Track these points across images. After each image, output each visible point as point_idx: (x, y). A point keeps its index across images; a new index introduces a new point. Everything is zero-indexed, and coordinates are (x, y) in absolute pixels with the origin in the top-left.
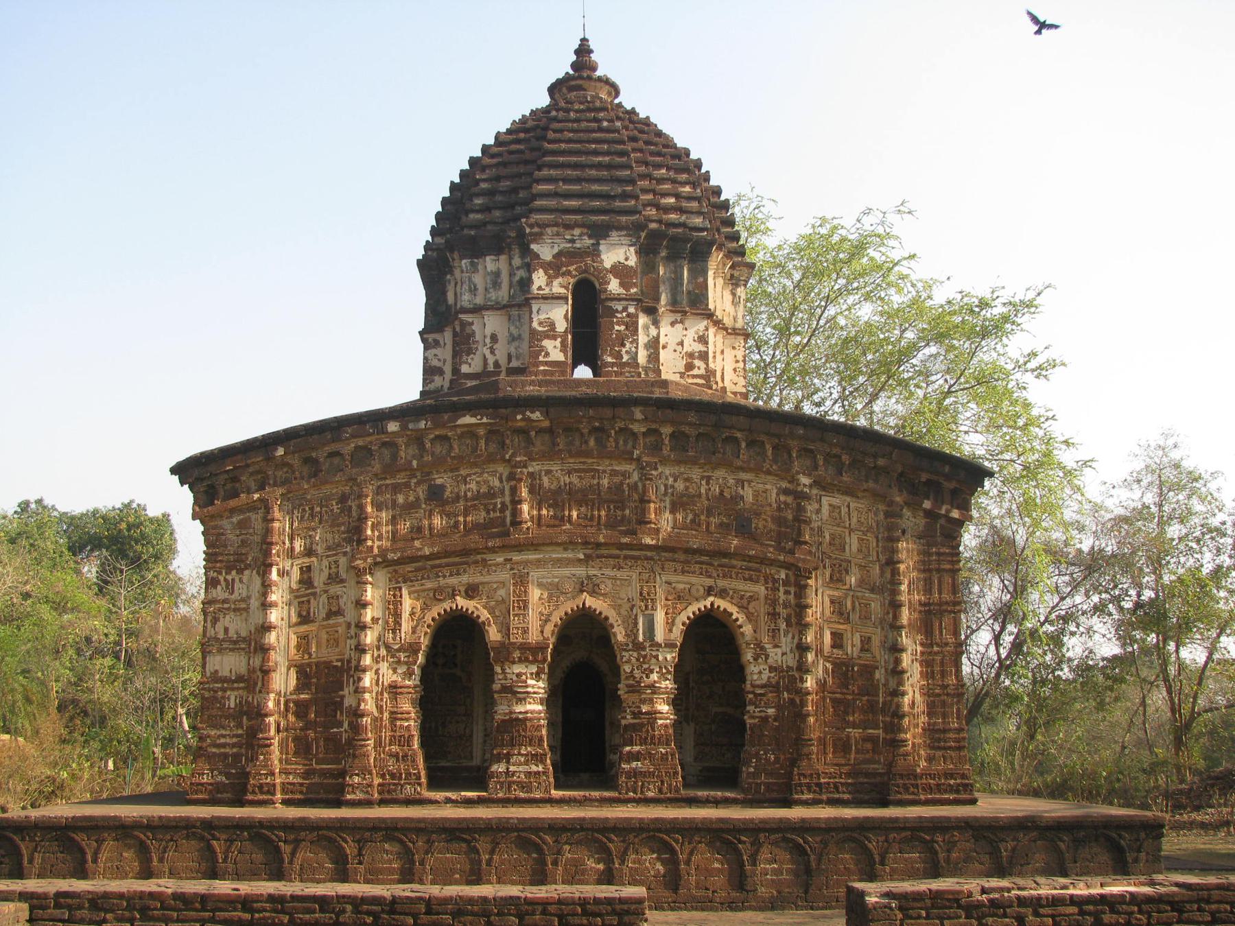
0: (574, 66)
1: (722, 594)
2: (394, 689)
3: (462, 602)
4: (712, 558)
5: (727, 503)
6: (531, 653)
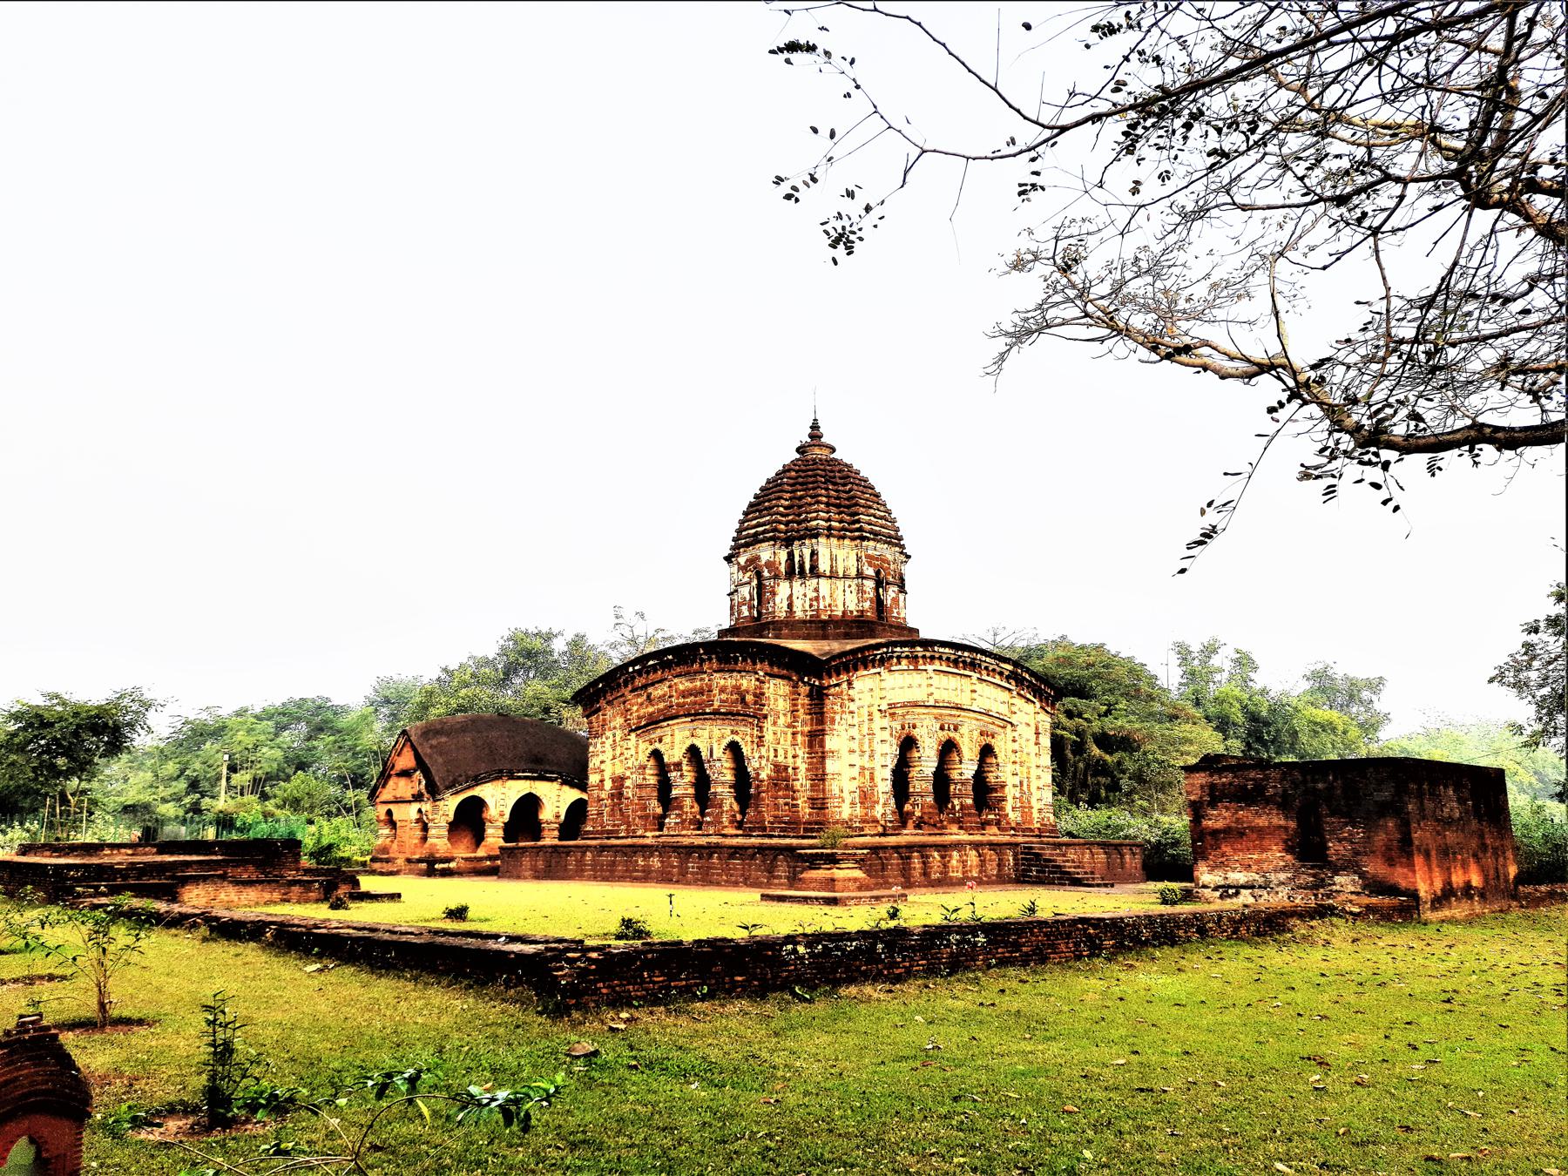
1: (737, 733)
2: (639, 786)
3: (657, 745)
4: (730, 715)
5: (737, 688)
6: (678, 766)
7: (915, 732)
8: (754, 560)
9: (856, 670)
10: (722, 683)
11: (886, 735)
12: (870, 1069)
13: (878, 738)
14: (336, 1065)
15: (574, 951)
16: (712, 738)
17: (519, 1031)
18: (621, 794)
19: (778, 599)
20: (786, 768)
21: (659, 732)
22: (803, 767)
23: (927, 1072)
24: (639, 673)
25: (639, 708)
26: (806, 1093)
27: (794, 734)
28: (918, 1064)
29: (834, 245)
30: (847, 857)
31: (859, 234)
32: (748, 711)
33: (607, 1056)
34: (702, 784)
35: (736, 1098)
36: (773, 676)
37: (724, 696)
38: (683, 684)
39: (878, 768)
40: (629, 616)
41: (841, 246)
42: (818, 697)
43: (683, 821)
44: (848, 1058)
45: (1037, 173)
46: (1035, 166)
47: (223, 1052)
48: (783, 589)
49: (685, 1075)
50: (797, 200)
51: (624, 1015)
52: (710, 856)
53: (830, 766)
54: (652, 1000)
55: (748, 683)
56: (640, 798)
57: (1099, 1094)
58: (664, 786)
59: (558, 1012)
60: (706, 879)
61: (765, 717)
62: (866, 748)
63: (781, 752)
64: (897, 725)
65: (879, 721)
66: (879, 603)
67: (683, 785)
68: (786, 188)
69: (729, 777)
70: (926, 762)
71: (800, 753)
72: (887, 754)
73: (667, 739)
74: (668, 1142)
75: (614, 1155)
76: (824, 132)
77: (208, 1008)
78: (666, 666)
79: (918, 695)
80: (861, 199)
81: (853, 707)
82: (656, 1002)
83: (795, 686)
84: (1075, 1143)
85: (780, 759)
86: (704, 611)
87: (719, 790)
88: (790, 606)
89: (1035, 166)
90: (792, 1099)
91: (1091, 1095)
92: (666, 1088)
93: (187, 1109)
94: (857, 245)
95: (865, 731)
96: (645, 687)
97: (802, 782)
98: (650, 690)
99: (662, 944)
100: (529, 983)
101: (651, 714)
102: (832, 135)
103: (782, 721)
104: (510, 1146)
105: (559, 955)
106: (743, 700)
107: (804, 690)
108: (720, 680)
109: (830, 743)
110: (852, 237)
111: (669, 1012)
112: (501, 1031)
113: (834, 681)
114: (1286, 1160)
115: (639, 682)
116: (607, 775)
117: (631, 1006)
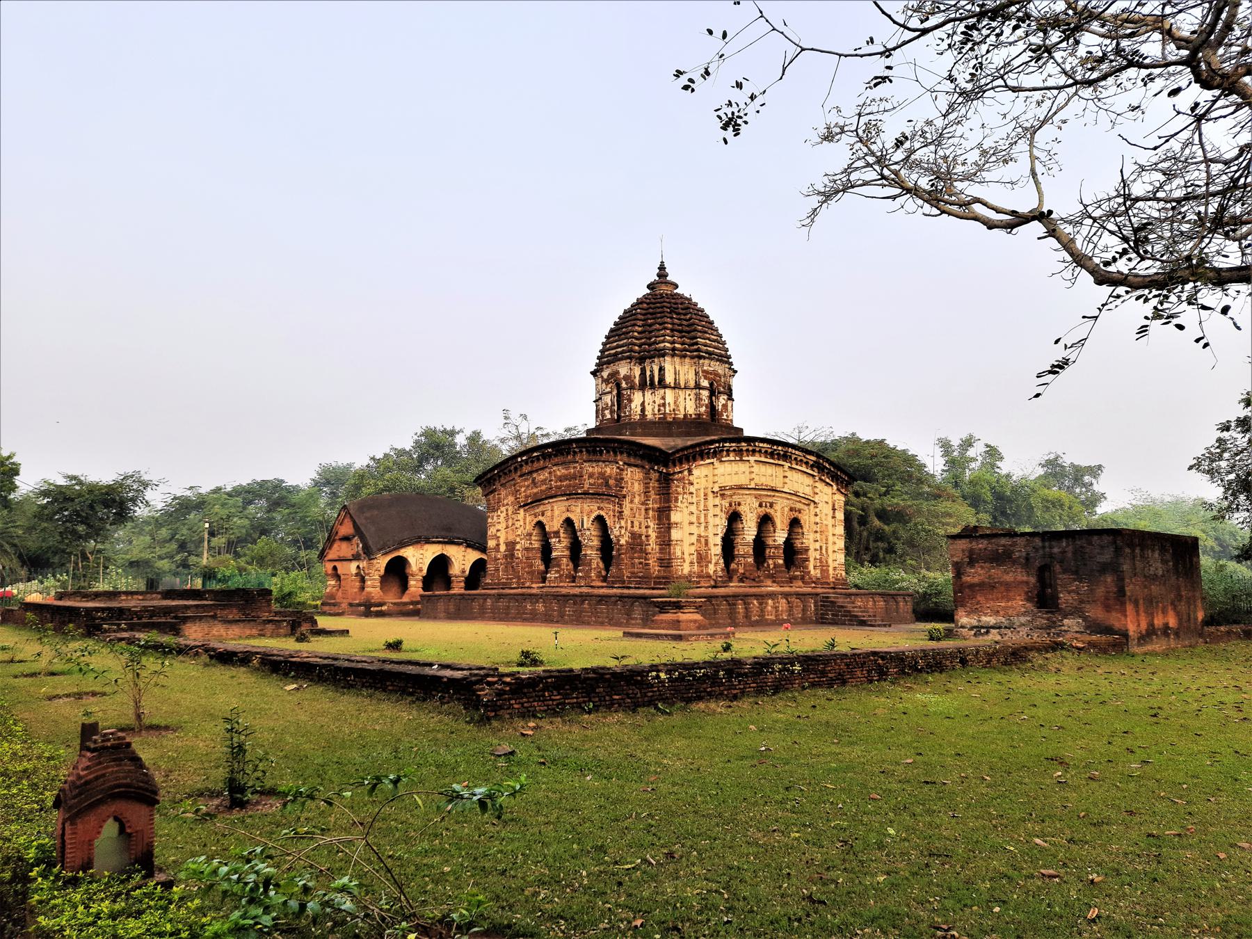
0: (658, 275)
2: (527, 549)
3: (541, 518)
5: (602, 475)
6: (557, 534)
7: (741, 509)
8: (614, 374)
9: (695, 460)
10: (591, 470)
11: (718, 509)
12: (720, 765)
13: (711, 514)
14: (320, 760)
15: (493, 676)
16: (584, 514)
17: (454, 736)
18: (512, 556)
19: (633, 405)
20: (640, 536)
21: (541, 508)
22: (653, 535)
23: (763, 769)
24: (526, 462)
25: (526, 489)
26: (674, 784)
27: (646, 510)
28: (755, 762)
29: (725, 128)
30: (689, 604)
31: (745, 118)
32: (611, 492)
33: (521, 755)
34: (575, 548)
35: (622, 787)
36: (629, 465)
37: (592, 481)
38: (561, 471)
39: (711, 535)
40: (515, 417)
41: (731, 129)
42: (666, 482)
43: (561, 576)
44: (702, 758)
45: (889, 68)
46: (888, 62)
47: (238, 751)
48: (637, 397)
49: (582, 770)
50: (693, 90)
51: (532, 724)
52: (583, 602)
53: (675, 534)
54: (553, 712)
55: (610, 470)
56: (528, 558)
57: (894, 786)
58: (546, 550)
59: (484, 721)
60: (579, 621)
61: (624, 497)
62: (702, 520)
63: (636, 524)
64: (726, 503)
65: (712, 500)
66: (712, 407)
67: (560, 548)
68: (683, 80)
69: (596, 542)
70: (749, 531)
71: (651, 524)
72: (718, 525)
73: (548, 513)
74: (575, 820)
75: (536, 830)
76: (718, 33)
77: (227, 720)
78: (545, 457)
79: (743, 480)
80: (748, 88)
81: (692, 489)
82: (555, 714)
83: (647, 473)
84: (881, 823)
85: (636, 529)
86: (573, 410)
87: (589, 552)
88: (643, 410)
89: (888, 62)
90: (664, 788)
91: (889, 787)
92: (569, 780)
93: (213, 794)
94: (743, 128)
95: (702, 507)
96: (531, 473)
97: (653, 546)
98: (535, 475)
99: (558, 671)
100: (459, 699)
101: (535, 494)
102: (725, 35)
103: (637, 500)
104: (457, 822)
105: (481, 680)
106: (607, 484)
107: (654, 476)
108: (589, 468)
109: (675, 517)
110: (739, 121)
111: (564, 722)
112: (440, 736)
113: (677, 469)
114: (1042, 835)
115: (526, 469)
116: (502, 541)
117: (535, 716)
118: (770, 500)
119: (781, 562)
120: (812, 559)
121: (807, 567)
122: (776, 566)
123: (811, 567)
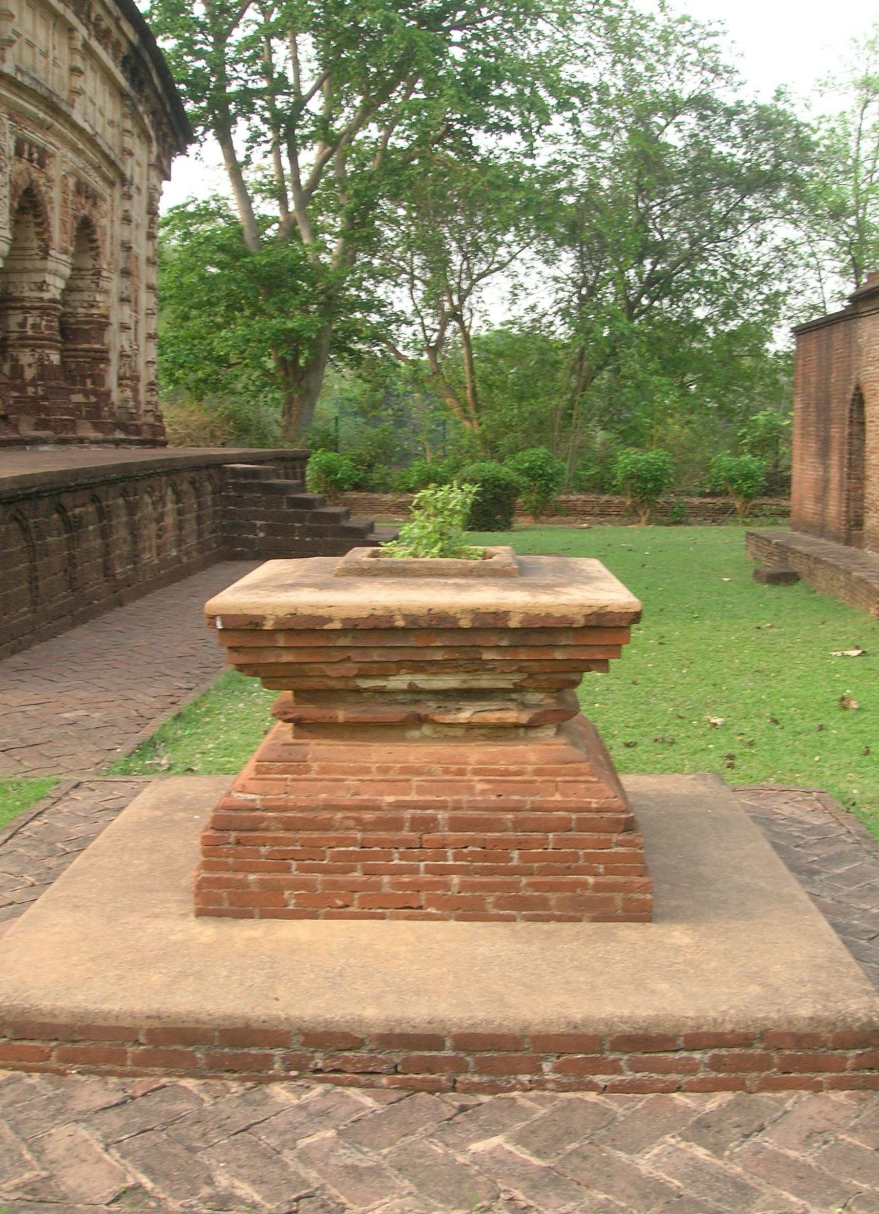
118: (37, 137)
119: (55, 358)
120: (114, 356)
121: (98, 380)
122: (44, 371)
123: (112, 380)
